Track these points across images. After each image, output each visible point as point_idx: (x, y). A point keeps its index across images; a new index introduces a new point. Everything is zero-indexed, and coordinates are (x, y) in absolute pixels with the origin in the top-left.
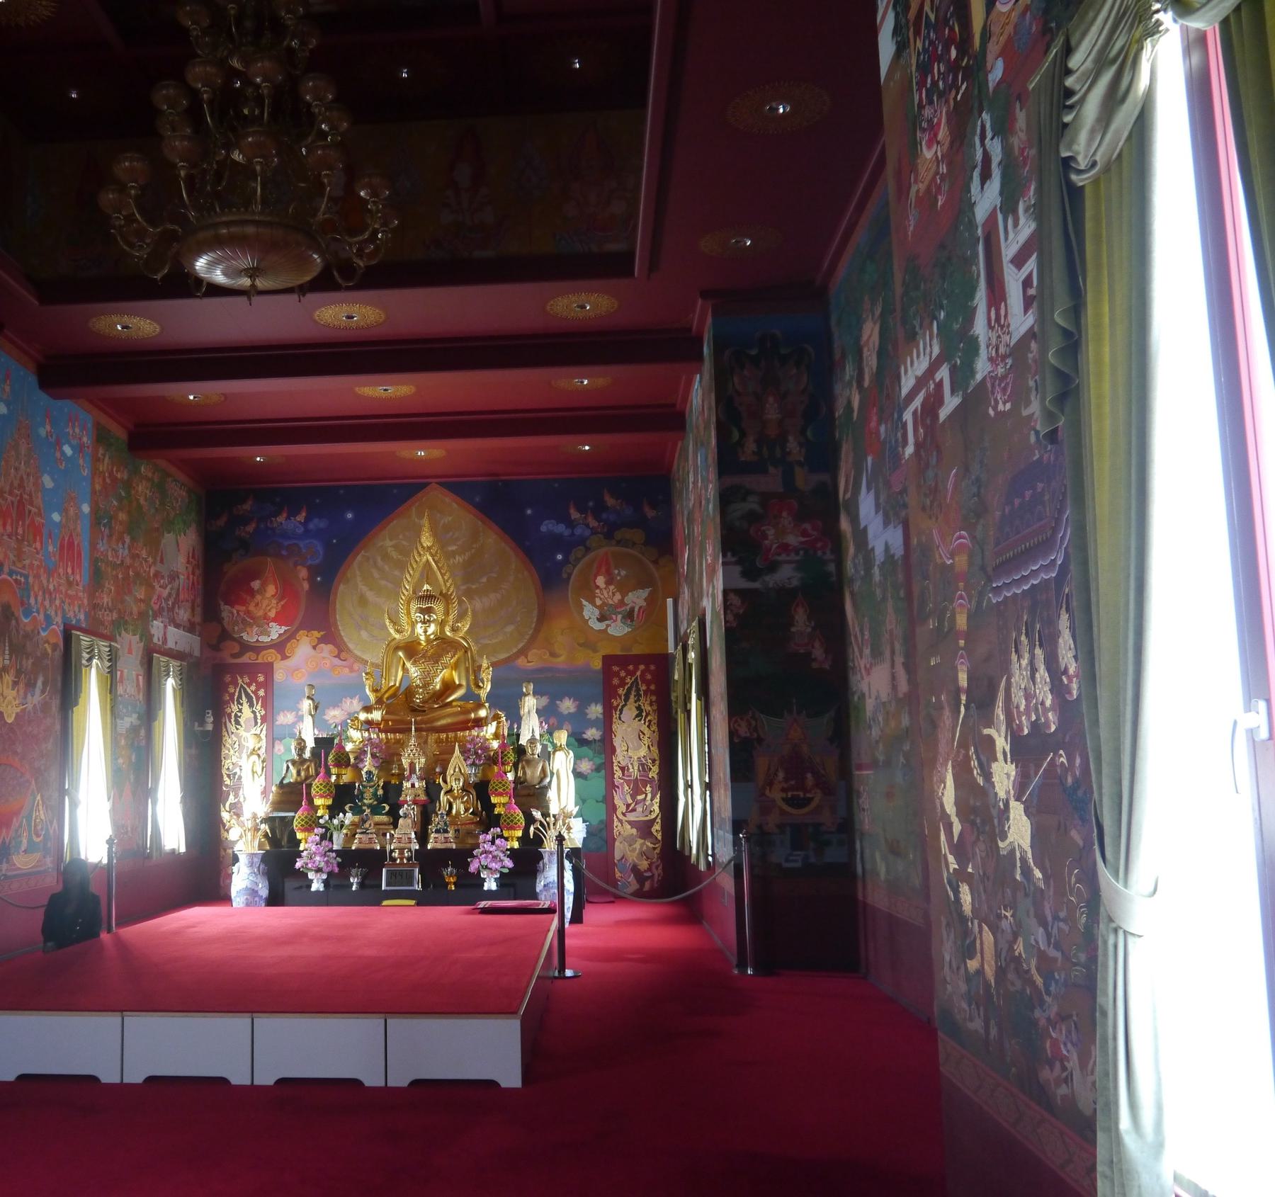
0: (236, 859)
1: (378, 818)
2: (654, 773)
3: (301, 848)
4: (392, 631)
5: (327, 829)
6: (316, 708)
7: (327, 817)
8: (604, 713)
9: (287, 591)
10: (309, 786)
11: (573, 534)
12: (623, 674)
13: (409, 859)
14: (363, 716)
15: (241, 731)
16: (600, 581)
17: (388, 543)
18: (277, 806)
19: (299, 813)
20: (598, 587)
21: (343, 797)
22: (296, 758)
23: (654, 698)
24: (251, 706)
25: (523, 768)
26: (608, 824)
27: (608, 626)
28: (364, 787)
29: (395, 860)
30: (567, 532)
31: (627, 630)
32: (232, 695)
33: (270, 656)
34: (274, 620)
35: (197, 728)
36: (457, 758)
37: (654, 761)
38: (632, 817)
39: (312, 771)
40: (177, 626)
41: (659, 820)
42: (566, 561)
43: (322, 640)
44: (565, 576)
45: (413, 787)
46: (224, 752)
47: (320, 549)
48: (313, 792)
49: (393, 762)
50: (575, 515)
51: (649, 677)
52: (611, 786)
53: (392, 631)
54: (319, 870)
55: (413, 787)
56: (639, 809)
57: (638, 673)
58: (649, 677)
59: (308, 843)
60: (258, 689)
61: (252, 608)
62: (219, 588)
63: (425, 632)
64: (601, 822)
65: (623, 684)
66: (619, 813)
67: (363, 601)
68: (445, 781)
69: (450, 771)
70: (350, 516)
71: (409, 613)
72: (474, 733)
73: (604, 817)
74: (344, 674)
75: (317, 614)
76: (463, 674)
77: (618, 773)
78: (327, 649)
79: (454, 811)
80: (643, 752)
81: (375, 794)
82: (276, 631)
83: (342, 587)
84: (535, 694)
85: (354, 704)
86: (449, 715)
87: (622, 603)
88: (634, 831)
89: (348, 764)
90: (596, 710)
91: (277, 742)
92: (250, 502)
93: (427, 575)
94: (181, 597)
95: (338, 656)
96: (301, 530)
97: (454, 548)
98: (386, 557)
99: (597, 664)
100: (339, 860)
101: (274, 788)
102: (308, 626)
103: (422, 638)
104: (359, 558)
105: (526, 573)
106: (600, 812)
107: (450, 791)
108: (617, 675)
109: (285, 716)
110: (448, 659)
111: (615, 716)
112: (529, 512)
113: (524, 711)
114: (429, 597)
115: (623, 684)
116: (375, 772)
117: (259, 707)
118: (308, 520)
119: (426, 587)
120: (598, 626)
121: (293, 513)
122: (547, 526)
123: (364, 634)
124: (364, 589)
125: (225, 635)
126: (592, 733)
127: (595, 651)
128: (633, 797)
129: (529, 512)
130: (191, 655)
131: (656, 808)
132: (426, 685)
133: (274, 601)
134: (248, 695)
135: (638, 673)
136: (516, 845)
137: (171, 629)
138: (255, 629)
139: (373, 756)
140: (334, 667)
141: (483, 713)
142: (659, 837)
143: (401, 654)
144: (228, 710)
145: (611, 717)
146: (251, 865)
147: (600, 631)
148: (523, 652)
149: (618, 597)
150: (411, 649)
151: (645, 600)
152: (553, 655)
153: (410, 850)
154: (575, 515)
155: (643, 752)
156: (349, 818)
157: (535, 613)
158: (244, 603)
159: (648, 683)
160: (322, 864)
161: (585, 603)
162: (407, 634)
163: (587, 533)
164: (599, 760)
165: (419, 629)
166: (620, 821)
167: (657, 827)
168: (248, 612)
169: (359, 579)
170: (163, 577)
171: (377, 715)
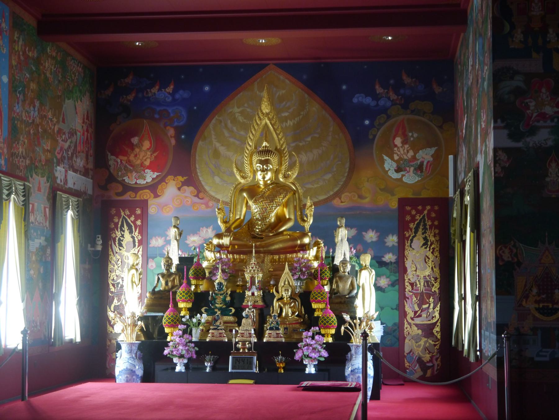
0: (119, 347)
1: (226, 318)
2: (436, 288)
3: (168, 340)
4: (238, 177)
5: (188, 326)
6: (180, 234)
7: (188, 317)
8: (399, 242)
9: (159, 145)
10: (175, 293)
11: (377, 105)
13: (250, 349)
14: (215, 241)
15: (124, 252)
16: (398, 141)
17: (236, 110)
18: (151, 307)
19: (167, 313)
20: (396, 146)
21: (200, 302)
22: (165, 272)
23: (437, 231)
24: (131, 232)
25: (337, 282)
26: (400, 326)
27: (403, 176)
28: (216, 294)
29: (238, 349)
30: (373, 103)
31: (418, 179)
33: (146, 194)
34: (148, 168)
35: (90, 248)
36: (286, 275)
37: (436, 279)
38: (418, 321)
39: (177, 282)
40: (75, 171)
41: (439, 324)
42: (372, 125)
43: (184, 184)
44: (371, 137)
45: (253, 295)
46: (110, 266)
47: (184, 113)
48: (178, 298)
49: (238, 276)
50: (379, 90)
51: (433, 215)
52: (403, 297)
53: (238, 177)
54: (181, 356)
55: (253, 295)
56: (424, 315)
57: (426, 212)
58: (433, 215)
59: (173, 336)
60: (136, 219)
61: (132, 158)
62: (106, 144)
63: (264, 178)
64: (395, 324)
65: (413, 220)
66: (408, 318)
67: (216, 154)
68: (277, 291)
69: (281, 284)
70: (207, 88)
71: (251, 164)
72: (300, 255)
73: (397, 321)
74: (202, 209)
75: (182, 164)
76: (292, 210)
77: (408, 288)
78: (189, 190)
79: (284, 314)
80: (428, 272)
81: (224, 300)
82: (150, 176)
83: (200, 143)
84: (347, 226)
85: (209, 232)
86: (281, 242)
87: (414, 158)
88: (420, 332)
89: (204, 277)
90: (392, 240)
91: (150, 260)
92: (131, 77)
93: (266, 134)
94: (78, 149)
95: (197, 196)
96: (169, 99)
97: (286, 114)
98: (234, 120)
99: (394, 205)
100: (197, 349)
101: (148, 295)
102: (175, 172)
103: (261, 182)
104: (214, 121)
105: (341, 134)
106: (395, 317)
107: (281, 299)
108: (409, 213)
109: (157, 240)
110: (282, 199)
111: (407, 244)
112: (344, 87)
113: (338, 239)
114: (267, 152)
115: (413, 220)
116: (225, 283)
117: (137, 233)
118: (175, 91)
119: (265, 144)
120: (395, 176)
121: (163, 86)
123: (217, 179)
124: (218, 145)
125: (111, 179)
126: (389, 257)
127: (393, 195)
128: (420, 306)
129: (344, 87)
130: (85, 193)
131: (437, 314)
132: (263, 219)
133: (149, 153)
135: (426, 212)
136: (330, 340)
137: (71, 173)
138: (134, 174)
139: (223, 271)
140: (194, 204)
141: (306, 240)
142: (439, 337)
143: (245, 194)
144: (114, 235)
145: (404, 245)
146: (130, 351)
147: (397, 180)
148: (337, 195)
149: (411, 153)
150: (253, 191)
151: (432, 156)
152: (361, 197)
153: (250, 343)
154: (379, 90)
155: (428, 272)
156: (205, 318)
157: (348, 165)
158: (125, 154)
159: (433, 220)
160: (184, 352)
161: (385, 157)
162: (249, 180)
163: (389, 104)
164: (394, 278)
165: (259, 176)
166: (409, 324)
167: (437, 329)
168: (129, 161)
170: (64, 133)
171: (226, 241)
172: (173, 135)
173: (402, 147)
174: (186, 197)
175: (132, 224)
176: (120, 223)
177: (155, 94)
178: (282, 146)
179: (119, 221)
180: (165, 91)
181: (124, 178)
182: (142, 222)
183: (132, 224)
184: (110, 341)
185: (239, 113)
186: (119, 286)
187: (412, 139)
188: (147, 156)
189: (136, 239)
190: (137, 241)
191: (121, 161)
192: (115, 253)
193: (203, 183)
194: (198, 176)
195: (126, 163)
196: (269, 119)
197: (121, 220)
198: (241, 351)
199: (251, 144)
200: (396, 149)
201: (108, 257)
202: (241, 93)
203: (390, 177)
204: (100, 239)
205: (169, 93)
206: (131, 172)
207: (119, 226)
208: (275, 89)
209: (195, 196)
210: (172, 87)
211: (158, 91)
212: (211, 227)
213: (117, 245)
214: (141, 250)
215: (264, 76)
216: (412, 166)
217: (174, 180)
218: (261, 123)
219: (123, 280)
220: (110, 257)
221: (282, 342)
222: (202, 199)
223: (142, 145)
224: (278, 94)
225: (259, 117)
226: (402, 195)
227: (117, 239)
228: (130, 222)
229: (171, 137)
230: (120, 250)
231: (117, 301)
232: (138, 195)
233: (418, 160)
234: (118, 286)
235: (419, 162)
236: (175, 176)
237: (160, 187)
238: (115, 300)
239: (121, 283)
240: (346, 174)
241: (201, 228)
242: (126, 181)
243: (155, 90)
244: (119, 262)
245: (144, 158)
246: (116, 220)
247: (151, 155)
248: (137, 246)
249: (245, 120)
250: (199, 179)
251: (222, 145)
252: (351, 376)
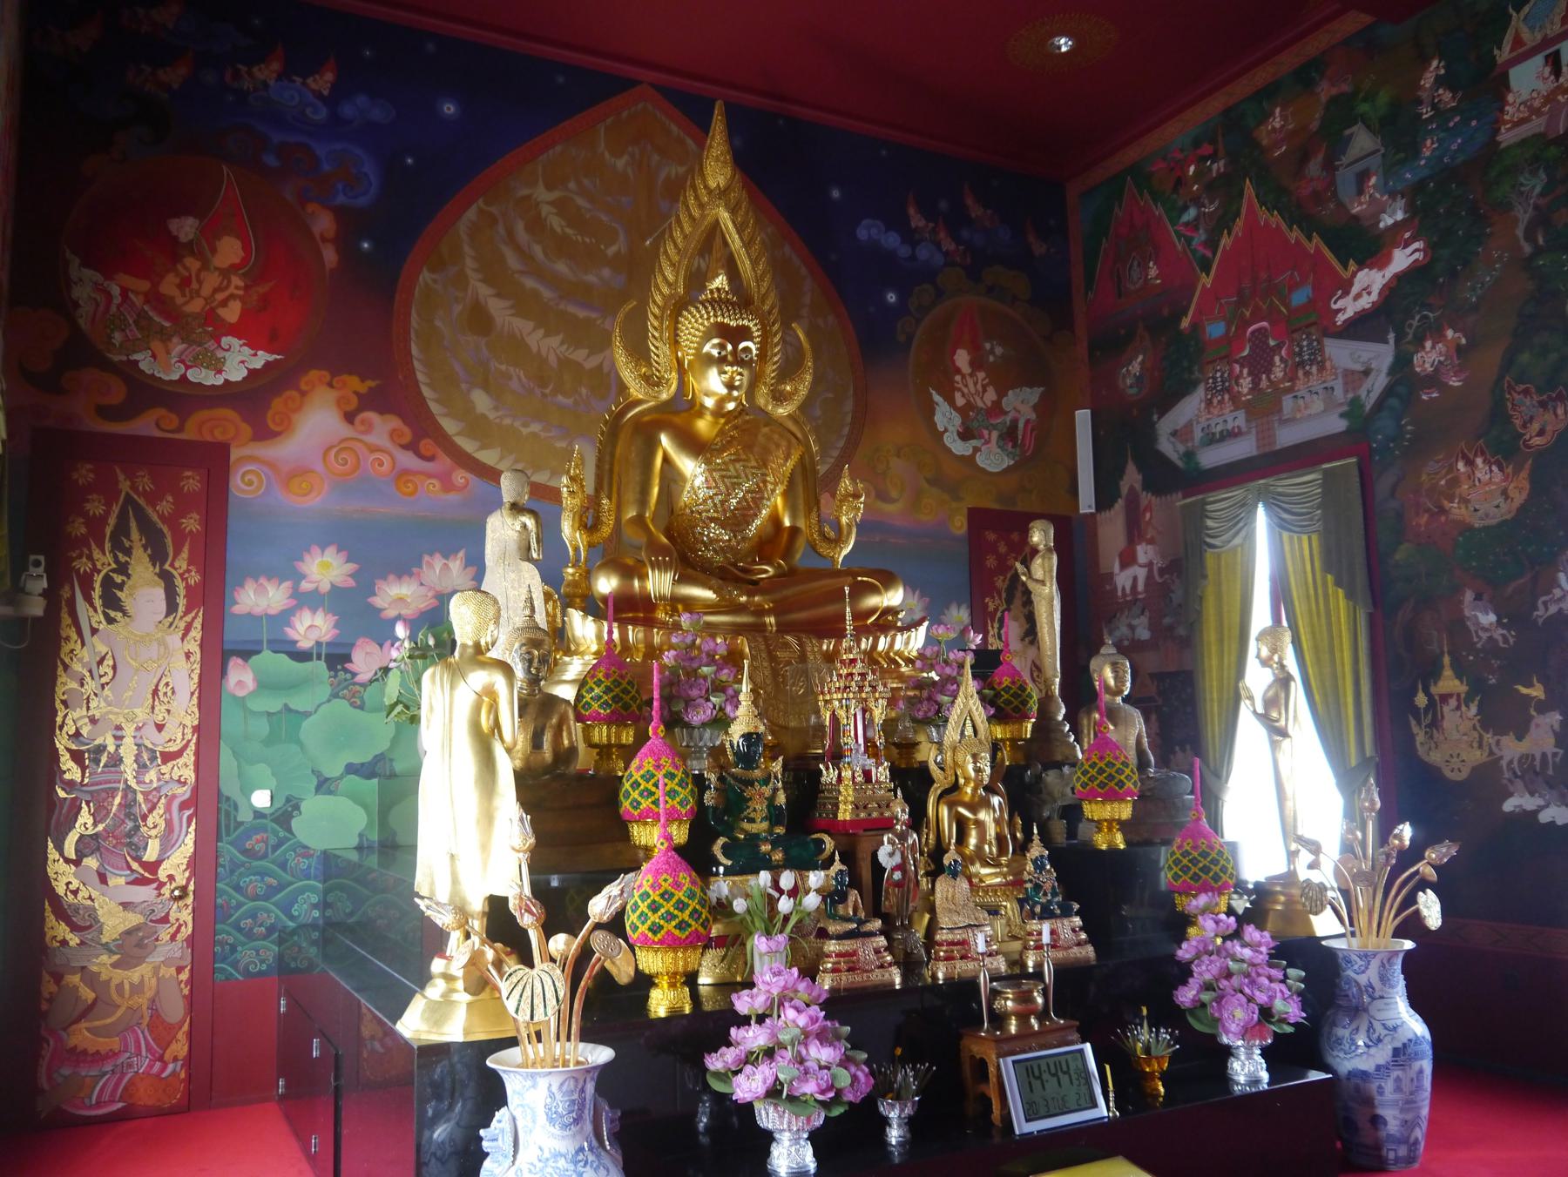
11: (913, 258)
12: (1002, 549)
16: (962, 358)
17: (542, 194)
20: (958, 371)
24: (158, 556)
27: (976, 450)
29: (999, 1019)
30: (904, 251)
31: (1007, 462)
32: (96, 525)
33: (222, 424)
34: (234, 331)
46: (65, 685)
50: (917, 221)
61: (169, 286)
67: (479, 320)
70: (449, 109)
78: (382, 428)
82: (239, 361)
83: (426, 276)
87: (996, 409)
91: (235, 664)
95: (412, 447)
96: (322, 114)
98: (537, 225)
99: (959, 525)
102: (338, 363)
104: (471, 214)
105: (831, 318)
109: (261, 590)
117: (182, 563)
120: (960, 448)
122: (868, 231)
123: (481, 401)
124: (484, 291)
134: (146, 527)
138: (178, 347)
144: (83, 565)
149: (991, 395)
154: (917, 221)
157: (849, 406)
161: (937, 398)
163: (939, 260)
168: (158, 300)
169: (470, 263)
172: (331, 234)
173: (971, 375)
174: (374, 449)
175: (165, 529)
176: (112, 521)
177: (266, 85)
178: (763, 303)
179: (108, 513)
180: (304, 84)
181: (135, 357)
182: (206, 522)
183: (165, 529)
184: (58, 978)
185: (551, 203)
186: (104, 759)
187: (991, 359)
188: (232, 290)
189: (178, 581)
190: (181, 590)
191: (124, 292)
192: (86, 632)
193: (435, 408)
194: (417, 382)
195: (147, 301)
196: (733, 212)
197: (116, 510)
199: (671, 278)
200: (958, 378)
201: (59, 648)
202: (558, 148)
203: (949, 451)
204: (41, 570)
205: (319, 95)
206: (165, 337)
207: (108, 531)
208: (656, 158)
209: (405, 447)
210: (329, 76)
211: (279, 78)
212: (461, 554)
213: (98, 602)
214: (198, 624)
215: (625, 114)
216: (995, 427)
217: (330, 385)
218: (703, 216)
219: (119, 738)
220: (66, 648)
221: (1087, 960)
222: (430, 459)
223: (214, 251)
224: (663, 175)
225: (697, 198)
226: (971, 501)
227: (98, 579)
228: (155, 518)
229: (324, 240)
230: (110, 621)
231: (90, 821)
232: (191, 424)
233: (1006, 413)
234: (97, 762)
235: (1008, 419)
236: (333, 375)
237: (277, 404)
238: (85, 817)
239: (111, 749)
240: (846, 430)
241: (426, 558)
242: (142, 366)
243: (267, 73)
244: (106, 668)
245: (220, 296)
246: (95, 507)
247: (247, 288)
248: (181, 609)
249: (569, 231)
250: (420, 393)
251: (499, 295)
252: (1396, 1073)
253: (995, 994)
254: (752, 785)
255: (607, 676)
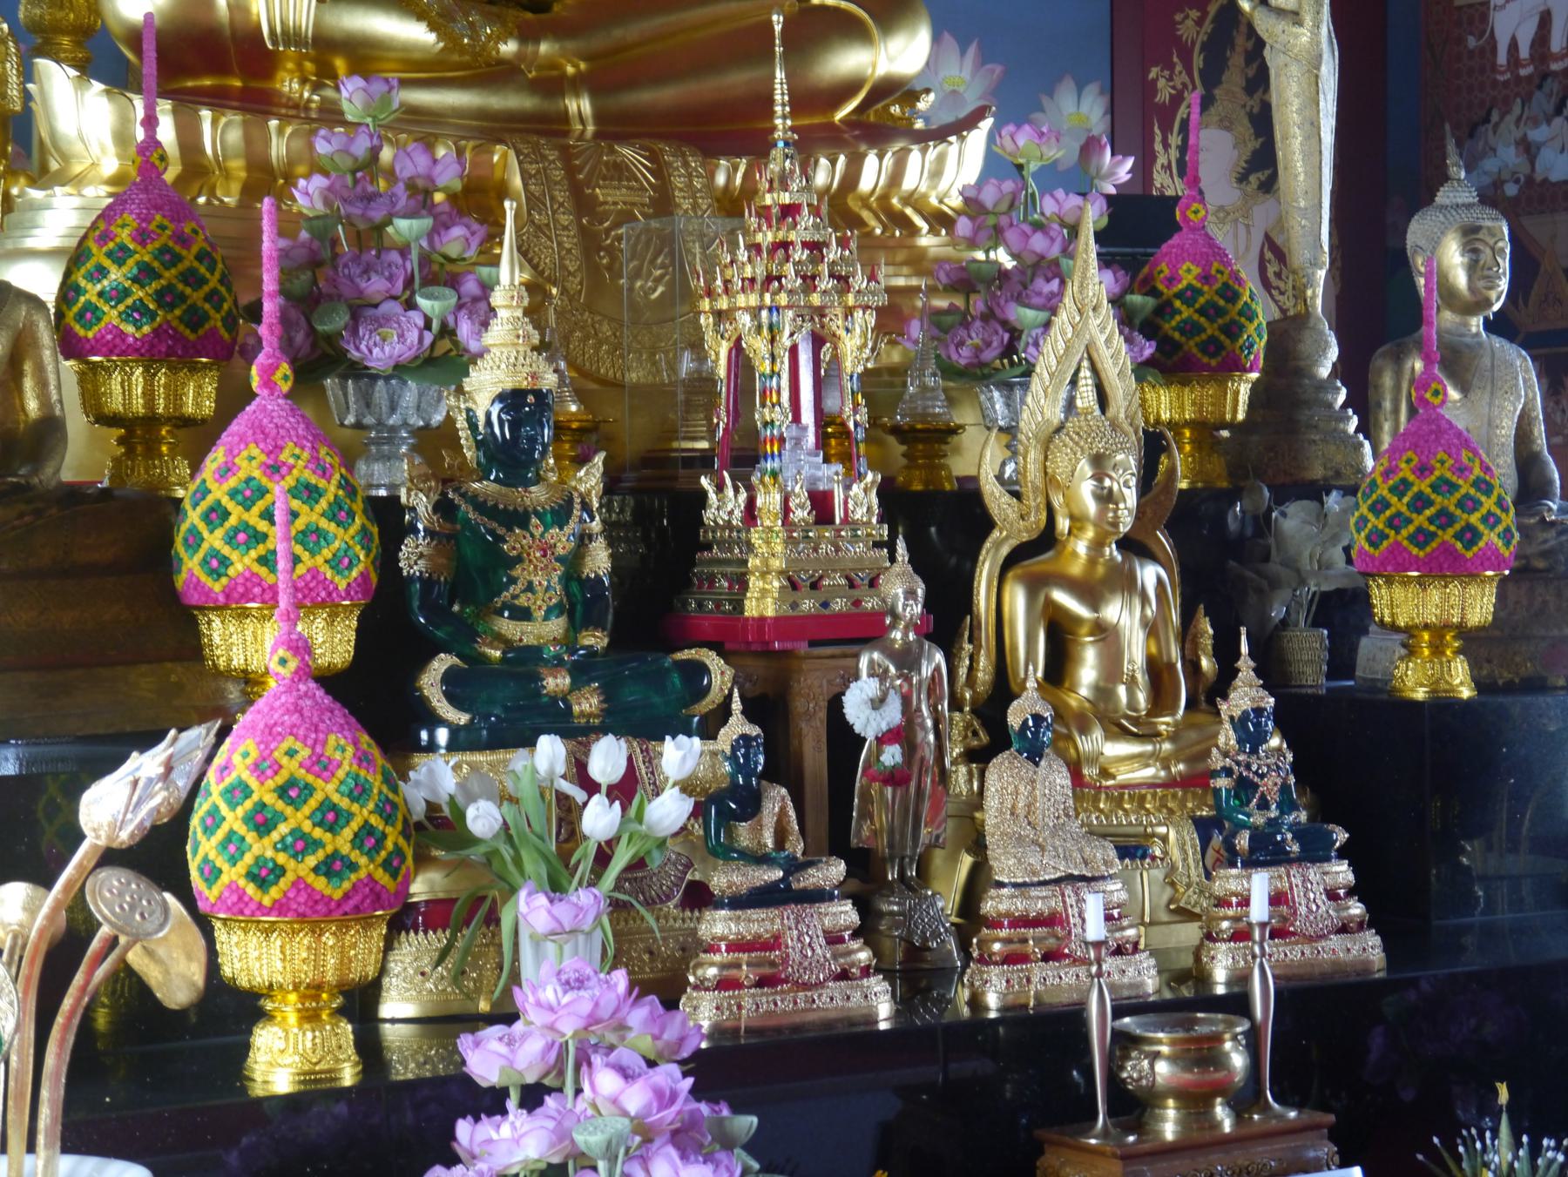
29: (1133, 1107)
198: (1169, 1127)
221: (1366, 967)
253: (1124, 1043)
254: (524, 525)
255: (142, 237)
